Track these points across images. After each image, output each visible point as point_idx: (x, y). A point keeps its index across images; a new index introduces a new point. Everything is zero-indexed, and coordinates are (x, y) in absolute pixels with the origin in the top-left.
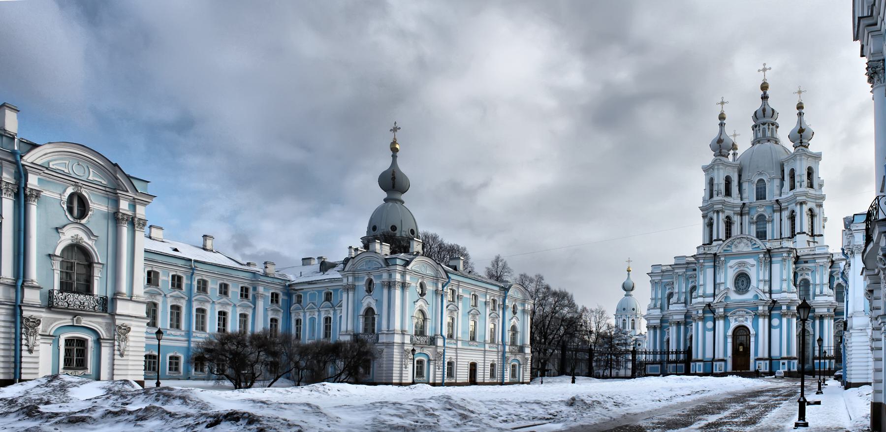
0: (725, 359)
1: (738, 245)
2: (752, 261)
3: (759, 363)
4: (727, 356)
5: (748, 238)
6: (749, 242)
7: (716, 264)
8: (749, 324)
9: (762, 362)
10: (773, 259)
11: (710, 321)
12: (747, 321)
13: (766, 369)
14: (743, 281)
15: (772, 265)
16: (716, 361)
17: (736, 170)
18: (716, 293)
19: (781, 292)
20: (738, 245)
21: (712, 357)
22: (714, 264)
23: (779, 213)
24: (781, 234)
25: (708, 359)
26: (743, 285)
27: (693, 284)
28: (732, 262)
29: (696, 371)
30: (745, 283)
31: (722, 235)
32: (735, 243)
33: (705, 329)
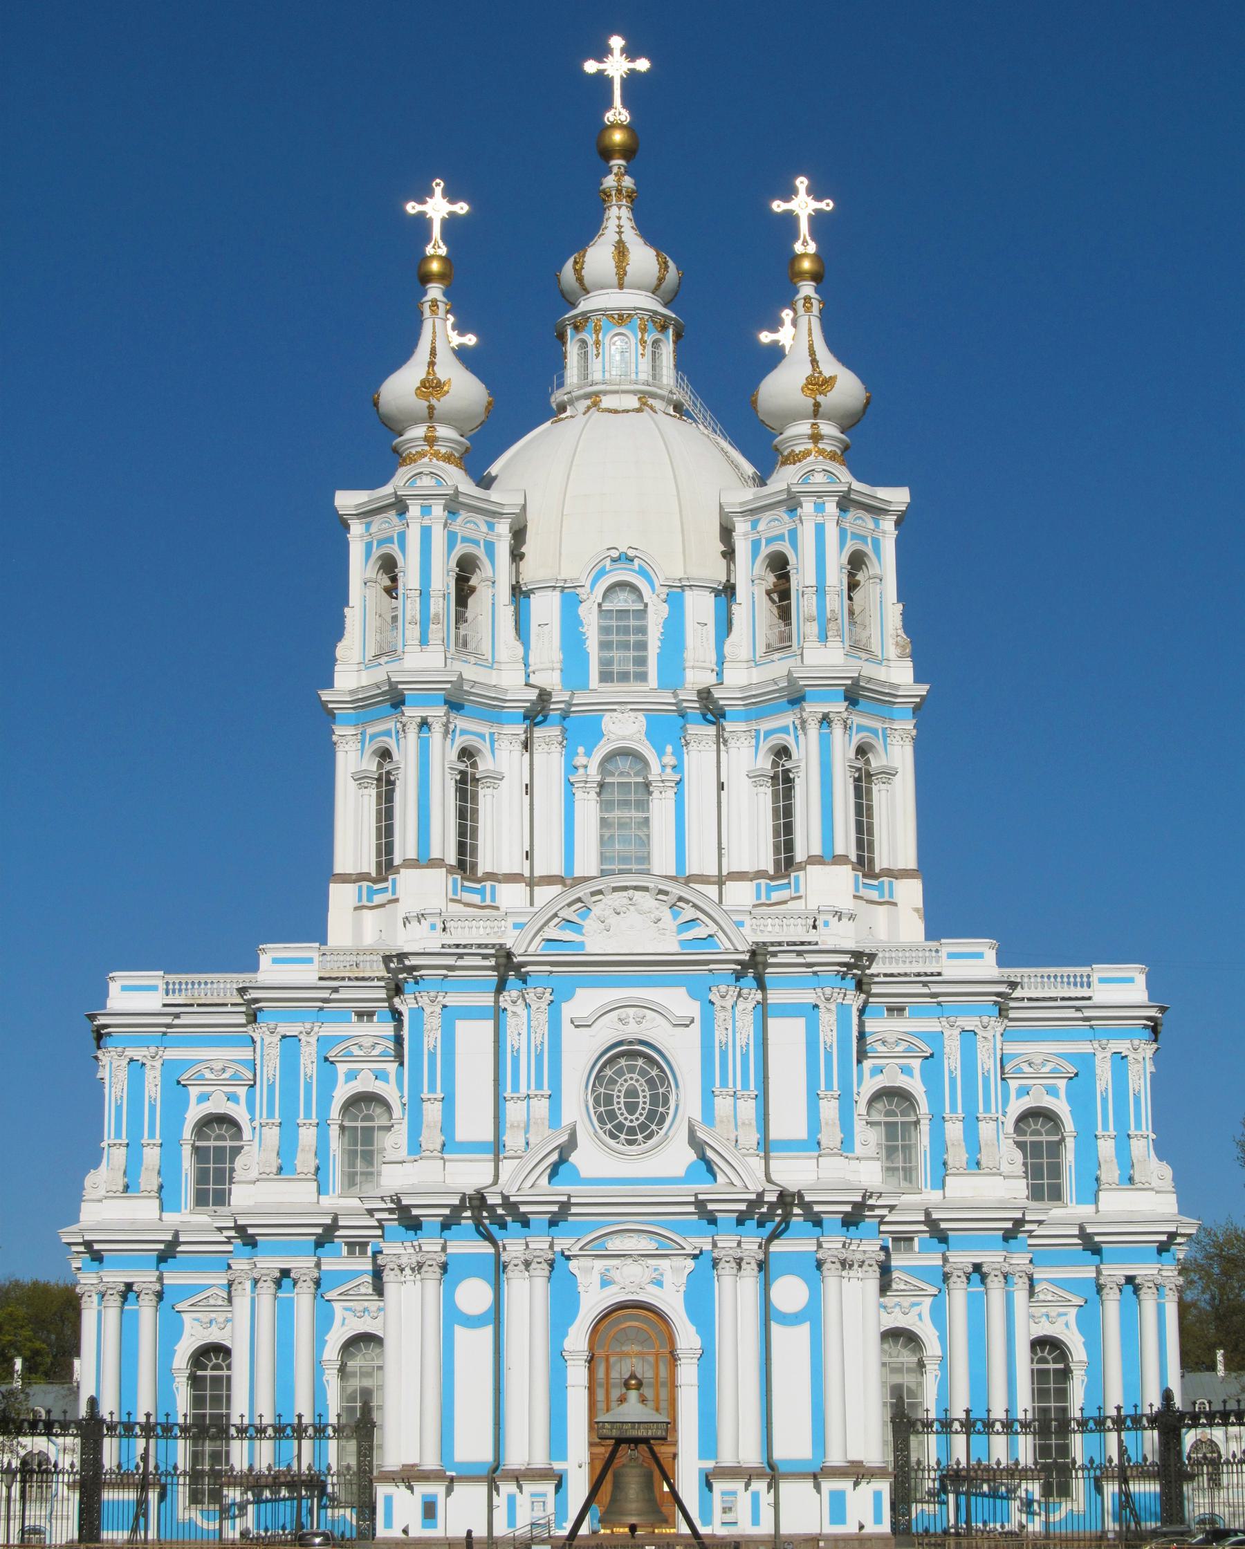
0: (558, 1466)
1: (613, 920)
2: (678, 1001)
3: (724, 1493)
4: (563, 1456)
5: (661, 892)
6: (666, 914)
7: (502, 1005)
8: (671, 1301)
9: (739, 1485)
10: (774, 997)
11: (484, 1278)
12: (659, 1283)
13: (756, 1521)
14: (631, 1093)
15: (771, 1022)
16: (518, 1477)
17: (503, 529)
18: (513, 1140)
19: (813, 1145)
20: (613, 920)
21: (487, 1456)
22: (497, 1001)
23: (715, 754)
24: (720, 856)
25: (462, 1464)
26: (632, 1108)
27: (358, 1086)
28: (585, 1002)
29: (405, 1531)
30: (644, 1100)
31: (445, 846)
32: (597, 910)
33: (452, 1317)
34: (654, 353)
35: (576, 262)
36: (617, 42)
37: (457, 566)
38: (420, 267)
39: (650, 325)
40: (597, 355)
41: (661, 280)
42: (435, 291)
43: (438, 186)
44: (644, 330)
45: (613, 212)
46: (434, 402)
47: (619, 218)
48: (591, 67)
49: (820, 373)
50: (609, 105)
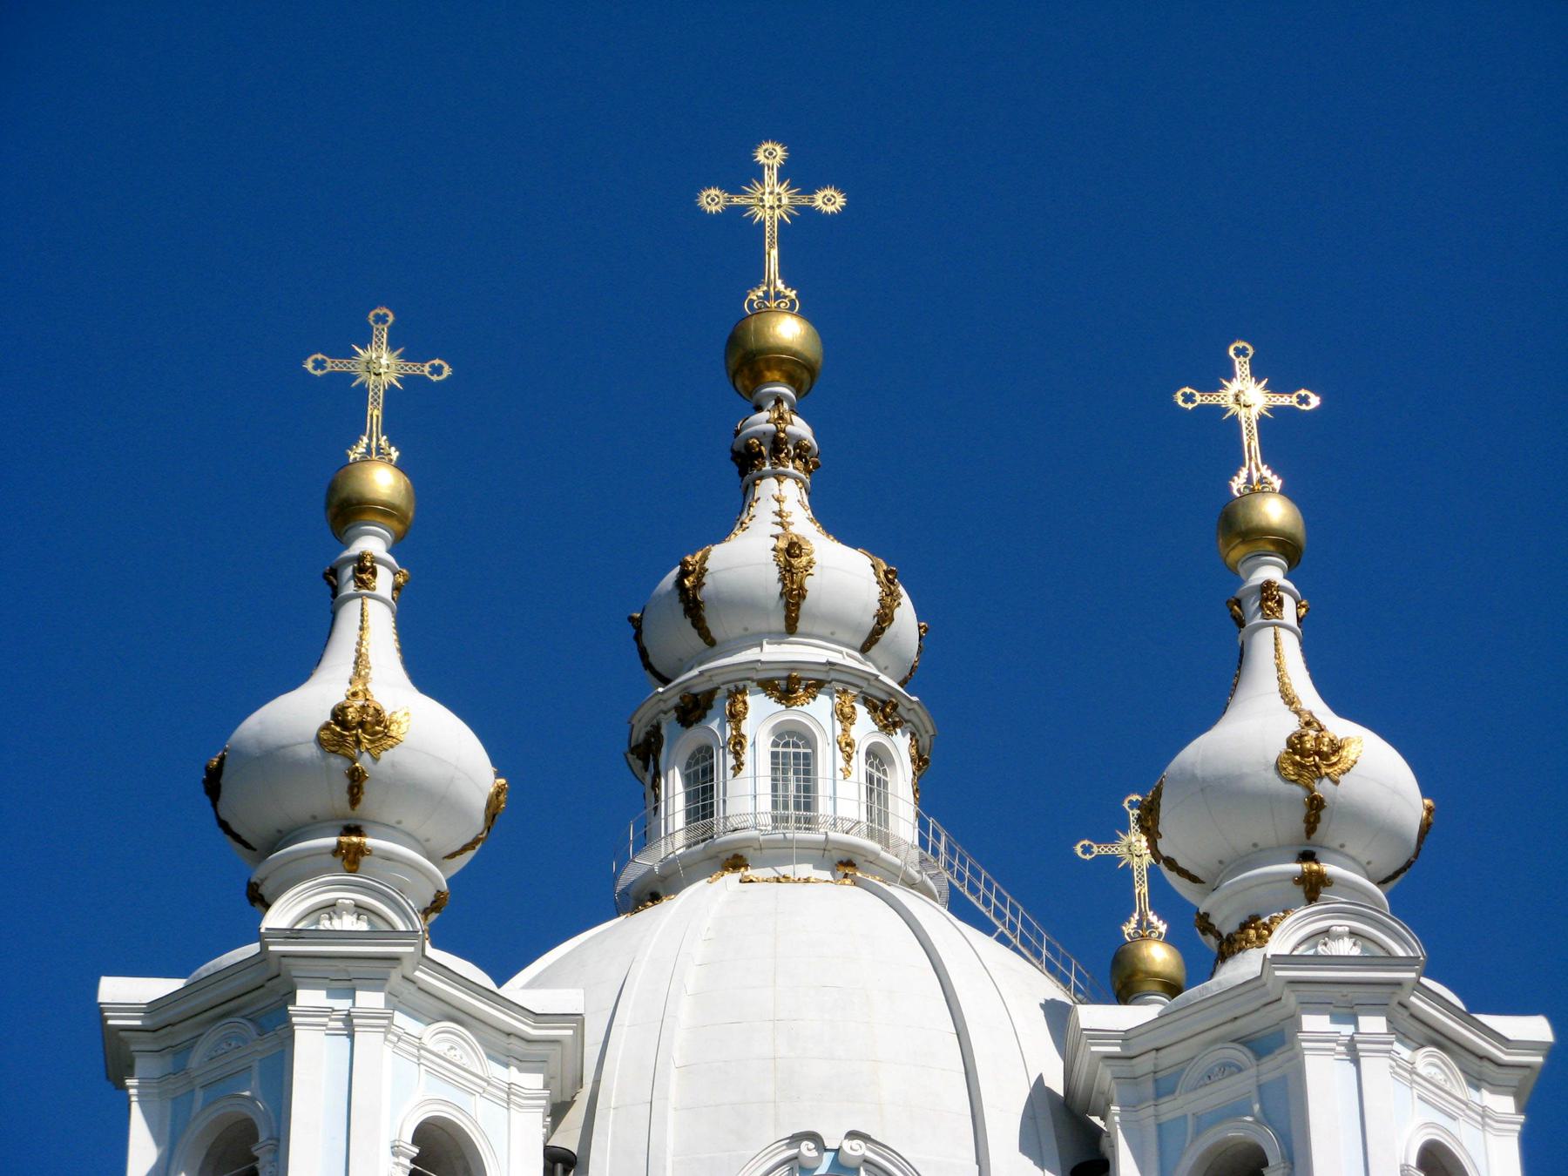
34: (870, 778)
35: (684, 574)
36: (771, 155)
37: (415, 1141)
38: (333, 489)
39: (862, 710)
40: (738, 767)
41: (884, 617)
42: (372, 543)
43: (381, 322)
44: (846, 718)
45: (767, 487)
46: (364, 762)
47: (778, 501)
48: (713, 200)
49: (1321, 729)
50: (756, 275)
